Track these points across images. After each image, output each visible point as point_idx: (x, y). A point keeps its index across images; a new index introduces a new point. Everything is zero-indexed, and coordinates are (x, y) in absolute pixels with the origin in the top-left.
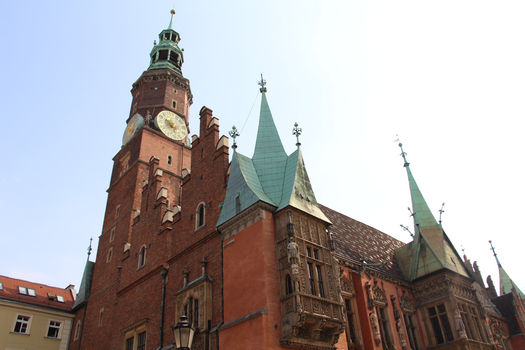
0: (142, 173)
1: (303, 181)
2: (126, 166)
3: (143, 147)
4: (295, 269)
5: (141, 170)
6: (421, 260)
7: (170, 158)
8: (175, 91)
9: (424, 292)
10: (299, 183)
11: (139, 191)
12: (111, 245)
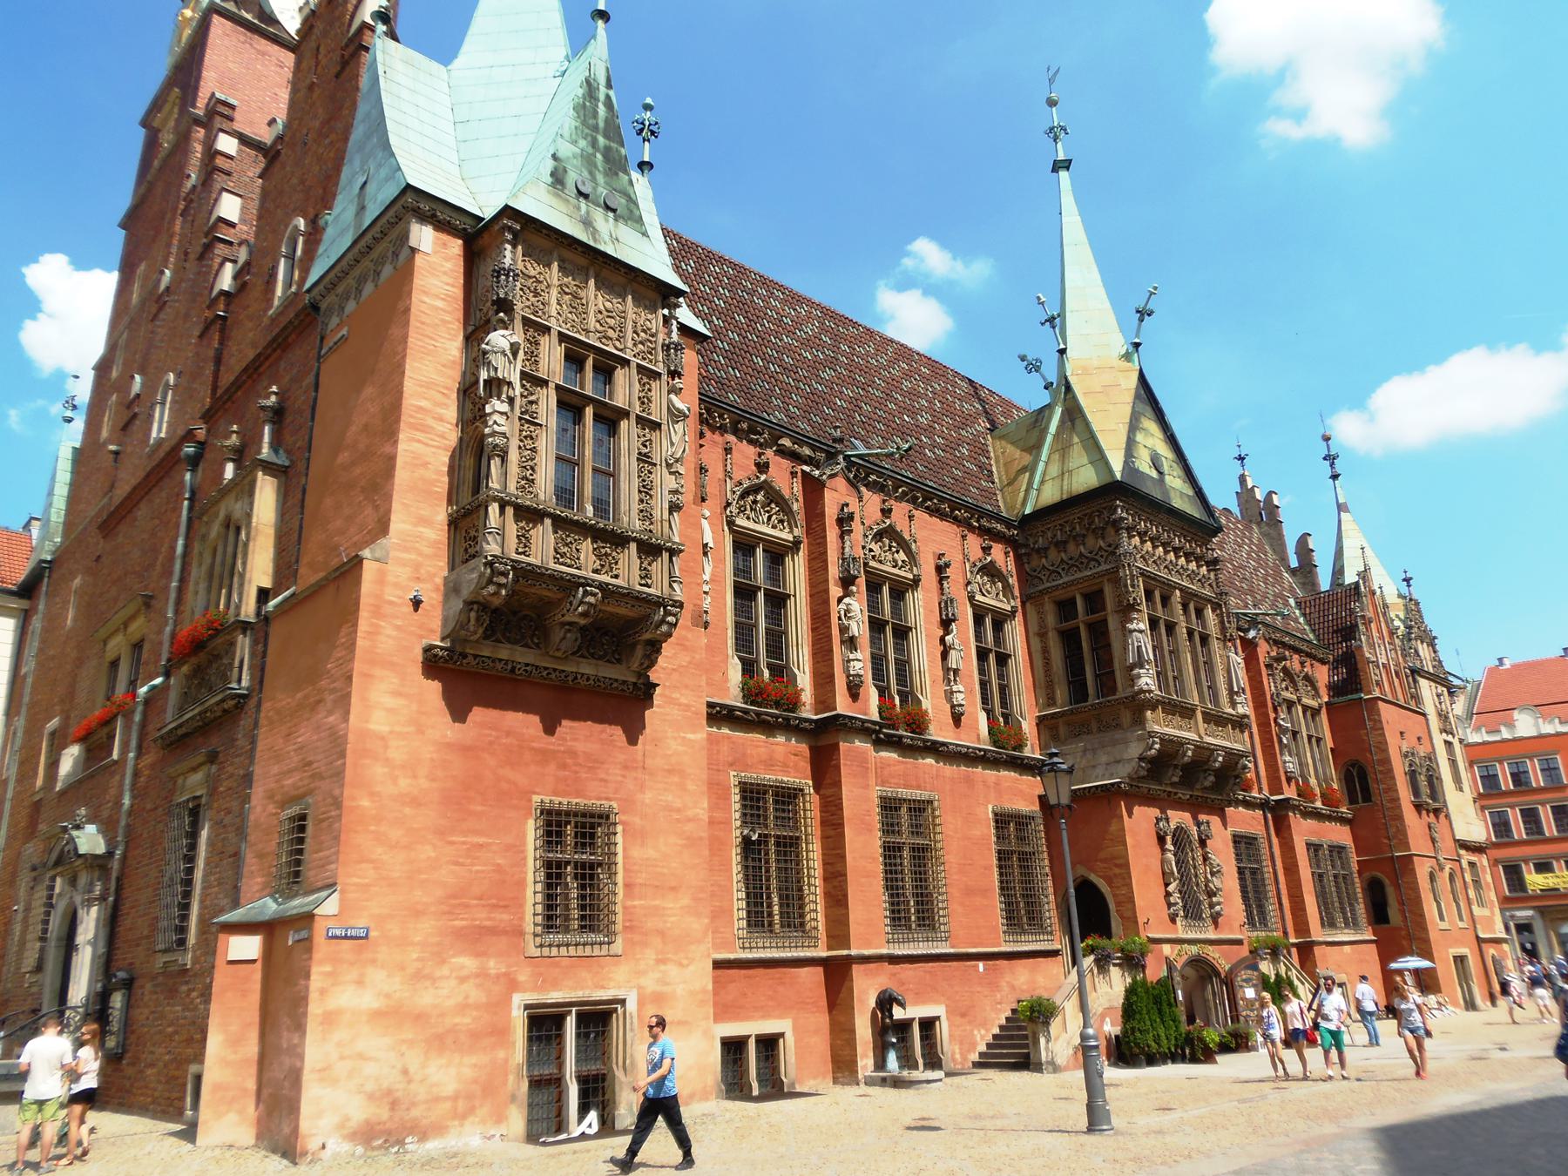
1: (594, 143)
4: (496, 417)
6: (1056, 456)
10: (574, 142)
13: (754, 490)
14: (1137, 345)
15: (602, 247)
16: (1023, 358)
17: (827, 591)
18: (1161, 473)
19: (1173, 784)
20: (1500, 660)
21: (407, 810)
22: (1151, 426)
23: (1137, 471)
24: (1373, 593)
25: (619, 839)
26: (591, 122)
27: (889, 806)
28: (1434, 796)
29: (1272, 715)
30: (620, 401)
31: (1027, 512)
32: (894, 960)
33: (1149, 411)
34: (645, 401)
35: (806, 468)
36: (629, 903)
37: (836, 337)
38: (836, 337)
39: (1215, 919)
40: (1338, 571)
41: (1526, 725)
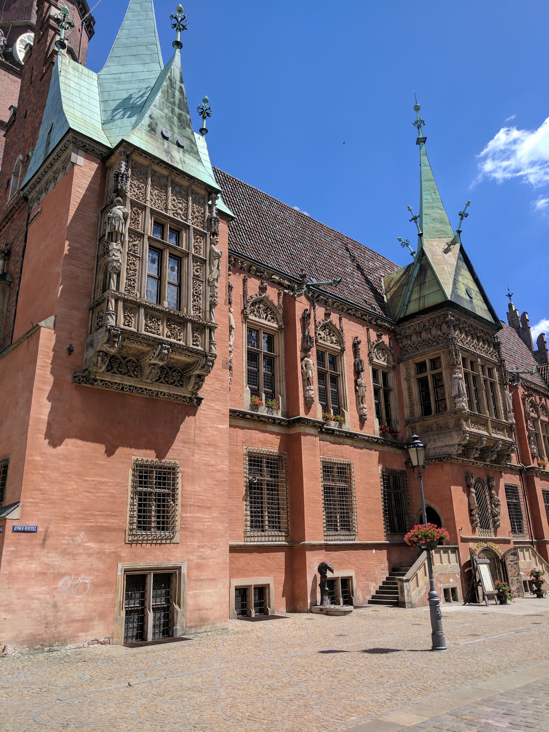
1: (173, 111)
6: (416, 289)
9: (414, 338)
10: (162, 110)
15: (175, 165)
16: (400, 240)
19: (476, 458)
21: (61, 463)
23: (459, 296)
25: (179, 480)
26: (172, 100)
31: (401, 317)
35: (286, 291)
36: (184, 515)
37: (304, 228)
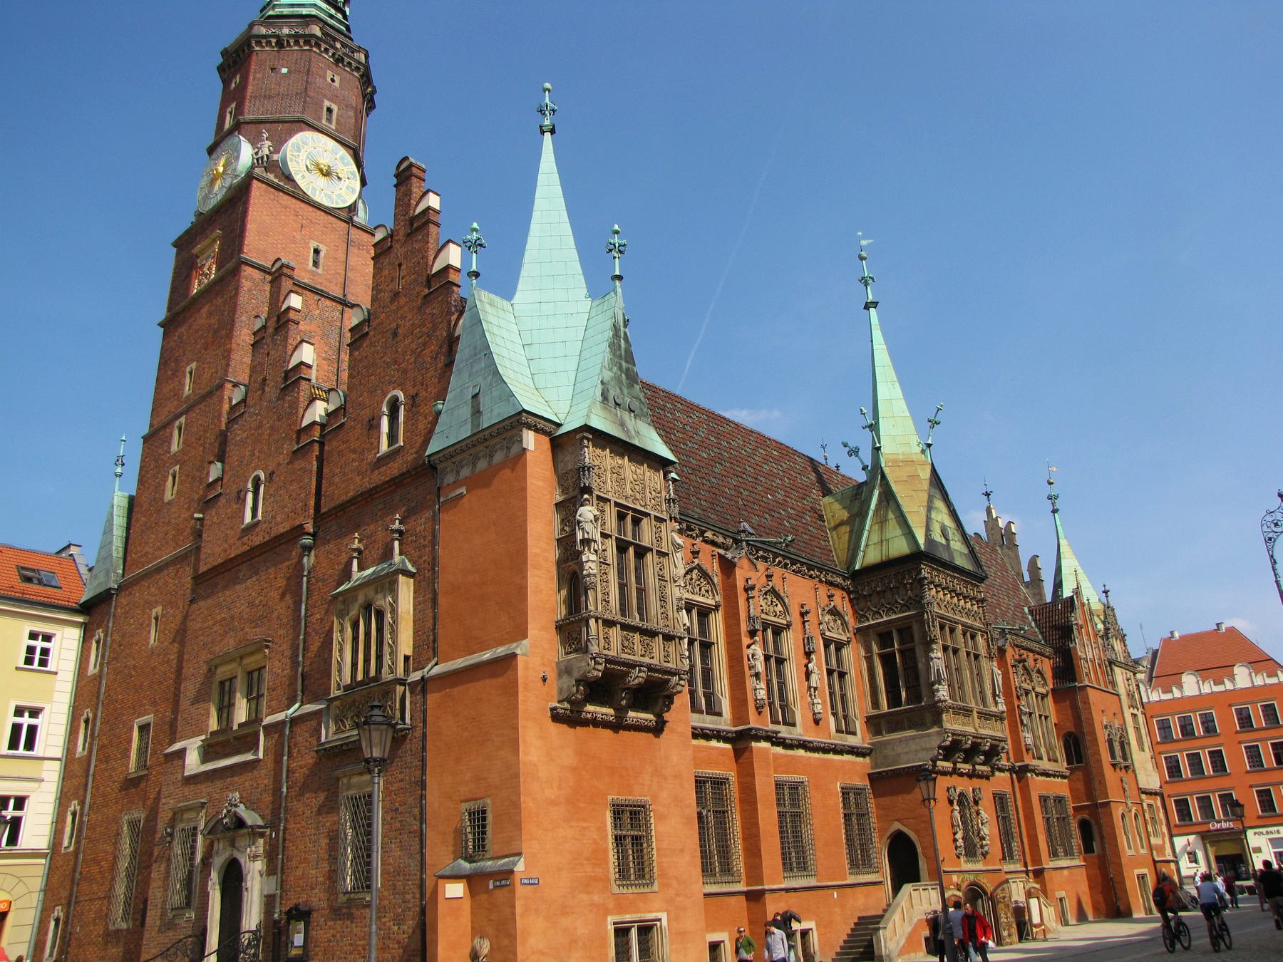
0: (250, 290)
1: (620, 367)
2: (210, 269)
3: (251, 227)
4: (589, 564)
5: (246, 285)
6: (876, 527)
7: (317, 251)
8: (333, 80)
10: (611, 370)
11: (244, 336)
12: (176, 459)
13: (691, 571)
14: (929, 446)
17: (740, 641)
18: (947, 540)
20: (1172, 633)
22: (939, 504)
24: (1083, 605)
27: (779, 786)
28: (1125, 758)
29: (1016, 703)
30: (646, 542)
31: (857, 568)
32: (787, 890)
33: (938, 496)
34: (659, 539)
35: (722, 552)
37: (719, 436)
38: (719, 436)
39: (984, 855)
40: (1058, 585)
41: (1190, 685)
